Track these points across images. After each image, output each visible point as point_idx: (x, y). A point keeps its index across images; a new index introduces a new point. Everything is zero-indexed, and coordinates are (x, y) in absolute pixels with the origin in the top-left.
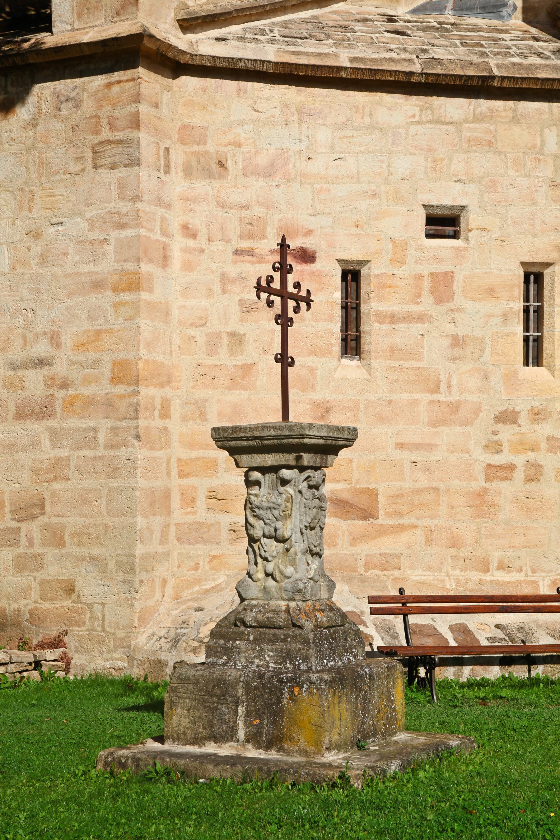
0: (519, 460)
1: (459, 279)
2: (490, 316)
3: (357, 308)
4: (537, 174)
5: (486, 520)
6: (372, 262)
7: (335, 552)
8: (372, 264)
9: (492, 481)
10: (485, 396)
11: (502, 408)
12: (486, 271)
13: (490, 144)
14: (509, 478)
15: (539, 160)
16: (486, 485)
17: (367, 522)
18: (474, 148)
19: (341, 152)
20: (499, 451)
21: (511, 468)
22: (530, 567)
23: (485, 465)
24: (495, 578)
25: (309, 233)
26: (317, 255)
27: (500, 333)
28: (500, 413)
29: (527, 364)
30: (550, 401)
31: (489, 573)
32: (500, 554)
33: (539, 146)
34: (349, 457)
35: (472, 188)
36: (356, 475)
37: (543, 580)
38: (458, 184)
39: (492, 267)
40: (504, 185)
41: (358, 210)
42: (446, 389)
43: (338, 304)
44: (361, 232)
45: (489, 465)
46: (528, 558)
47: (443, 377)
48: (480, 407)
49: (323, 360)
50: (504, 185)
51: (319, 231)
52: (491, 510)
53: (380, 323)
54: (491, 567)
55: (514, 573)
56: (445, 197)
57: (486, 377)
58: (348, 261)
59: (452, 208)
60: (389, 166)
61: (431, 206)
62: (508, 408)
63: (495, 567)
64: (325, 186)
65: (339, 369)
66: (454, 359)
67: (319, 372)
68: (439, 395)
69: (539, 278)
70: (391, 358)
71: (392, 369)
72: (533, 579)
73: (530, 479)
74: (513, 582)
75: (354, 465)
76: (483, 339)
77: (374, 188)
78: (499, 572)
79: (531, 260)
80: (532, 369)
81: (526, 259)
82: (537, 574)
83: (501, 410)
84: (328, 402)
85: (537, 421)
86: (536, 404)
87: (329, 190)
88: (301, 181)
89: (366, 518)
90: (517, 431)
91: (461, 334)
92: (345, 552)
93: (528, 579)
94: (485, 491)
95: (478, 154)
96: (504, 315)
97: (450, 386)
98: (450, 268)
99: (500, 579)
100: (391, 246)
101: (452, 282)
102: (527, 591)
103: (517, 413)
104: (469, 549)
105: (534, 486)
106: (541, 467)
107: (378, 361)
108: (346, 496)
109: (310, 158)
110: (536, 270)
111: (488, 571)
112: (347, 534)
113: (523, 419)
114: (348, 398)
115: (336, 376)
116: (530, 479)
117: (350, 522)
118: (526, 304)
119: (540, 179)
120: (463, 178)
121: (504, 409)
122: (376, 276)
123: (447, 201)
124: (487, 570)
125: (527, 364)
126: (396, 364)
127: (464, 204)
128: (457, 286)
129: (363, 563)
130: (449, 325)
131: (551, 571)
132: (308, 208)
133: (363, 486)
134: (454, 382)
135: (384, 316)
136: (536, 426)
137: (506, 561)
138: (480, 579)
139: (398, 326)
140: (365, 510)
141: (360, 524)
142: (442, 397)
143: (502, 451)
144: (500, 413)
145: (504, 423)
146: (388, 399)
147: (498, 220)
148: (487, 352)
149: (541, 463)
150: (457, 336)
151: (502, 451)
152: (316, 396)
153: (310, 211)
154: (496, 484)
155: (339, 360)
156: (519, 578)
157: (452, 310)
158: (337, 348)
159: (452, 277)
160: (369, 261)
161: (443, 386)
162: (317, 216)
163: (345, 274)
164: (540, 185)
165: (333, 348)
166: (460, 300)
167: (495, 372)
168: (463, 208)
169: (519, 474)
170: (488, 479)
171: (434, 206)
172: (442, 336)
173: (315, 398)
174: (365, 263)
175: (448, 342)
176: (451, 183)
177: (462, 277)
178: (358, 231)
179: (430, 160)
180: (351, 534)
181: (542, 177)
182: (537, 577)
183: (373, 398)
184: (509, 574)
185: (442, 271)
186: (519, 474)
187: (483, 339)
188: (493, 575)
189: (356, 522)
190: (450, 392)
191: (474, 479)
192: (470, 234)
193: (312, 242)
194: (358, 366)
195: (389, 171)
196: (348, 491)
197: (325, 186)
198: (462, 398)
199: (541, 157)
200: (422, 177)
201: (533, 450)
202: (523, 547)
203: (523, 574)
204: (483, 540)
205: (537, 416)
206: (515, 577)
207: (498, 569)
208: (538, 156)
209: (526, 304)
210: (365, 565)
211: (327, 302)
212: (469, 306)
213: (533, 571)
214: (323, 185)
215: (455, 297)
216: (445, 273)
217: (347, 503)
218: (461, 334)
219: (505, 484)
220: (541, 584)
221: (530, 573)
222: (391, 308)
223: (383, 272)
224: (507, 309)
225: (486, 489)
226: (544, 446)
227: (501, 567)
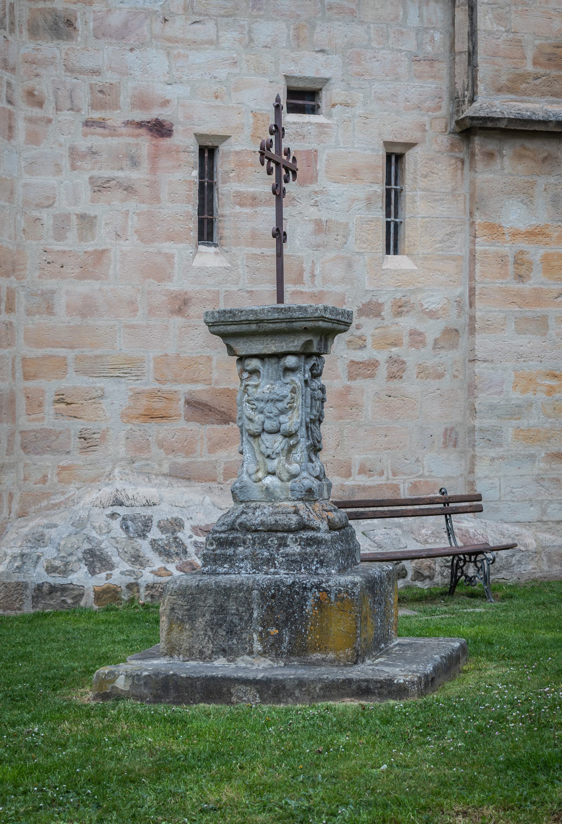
0: (382, 356)
1: (323, 157)
2: (354, 200)
3: (211, 186)
4: (400, 47)
5: (349, 421)
6: (232, 138)
7: (193, 460)
8: (232, 140)
9: (355, 379)
10: (349, 287)
11: (366, 300)
12: (349, 150)
13: (352, 12)
14: (372, 376)
15: (402, 33)
16: (349, 383)
17: (227, 426)
18: (337, 16)
19: (200, 14)
20: (362, 347)
21: (374, 364)
22: (391, 469)
23: (348, 362)
24: (357, 483)
25: (166, 103)
26: (174, 128)
27: (364, 218)
28: (363, 305)
29: (388, 252)
30: (413, 292)
31: (351, 478)
32: (362, 457)
33: (401, 17)
34: (208, 355)
35: (336, 59)
36: (215, 375)
37: (404, 483)
38: (319, 55)
39: (356, 146)
40: (368, 58)
41: (217, 80)
42: (310, 279)
43: (195, 184)
44: (221, 104)
45: (352, 361)
46: (389, 461)
47: (307, 266)
48: (344, 298)
49: (181, 246)
50: (368, 58)
51: (176, 101)
52: (354, 410)
53: (241, 205)
54: (353, 471)
55: (376, 476)
56: (308, 67)
57: (350, 265)
58: (206, 136)
59: (314, 80)
60: (250, 32)
61: (293, 77)
62: (371, 300)
63: (357, 471)
64: (182, 51)
65: (197, 256)
66: (317, 247)
67: (176, 259)
68: (302, 286)
69: (400, 157)
70: (252, 244)
71: (254, 257)
72: (395, 482)
73: (392, 377)
74: (374, 487)
75: (214, 363)
76: (347, 224)
77: (235, 55)
78: (360, 476)
79: (395, 140)
80: (391, 257)
81: (390, 138)
82: (398, 478)
83: (364, 302)
84: (186, 293)
85: (399, 314)
86: (399, 295)
87: (187, 56)
88: (157, 46)
89: (226, 422)
90: (380, 325)
91: (324, 219)
92: (204, 459)
93: (389, 482)
94: (348, 389)
95: (340, 23)
96: (369, 199)
97: (313, 276)
98: (314, 146)
99: (361, 483)
100: (251, 121)
101: (316, 161)
102: (388, 495)
103: (382, 304)
104: (332, 452)
105: (395, 384)
106: (404, 363)
107: (239, 248)
108: (205, 398)
109: (166, 20)
110: (397, 150)
111: (350, 476)
112: (206, 440)
113: (387, 311)
114: (208, 288)
115: (194, 264)
116: (392, 377)
117: (209, 427)
118: (388, 187)
119: (403, 53)
120: (326, 48)
121: (368, 300)
122: (237, 153)
123: (310, 73)
124: (348, 475)
125: (388, 252)
126: (258, 251)
127: (327, 77)
128: (321, 166)
129: (222, 471)
130: (312, 209)
131: (412, 474)
132: (164, 76)
133: (222, 386)
134: (317, 272)
135: (245, 197)
136: (398, 320)
137: (368, 465)
138: (342, 485)
139: (259, 209)
140: (225, 413)
141: (221, 429)
142: (305, 289)
143: (365, 346)
144: (363, 305)
145: (367, 316)
146: (249, 289)
147: (362, 95)
148: (351, 239)
149: (404, 359)
150: (320, 220)
151: (365, 346)
152: (173, 286)
153: (167, 79)
154: (358, 383)
155: (197, 248)
156: (380, 482)
157: (316, 192)
158: (194, 234)
159: (316, 156)
160: (229, 137)
161: (306, 275)
162: (174, 85)
163: (202, 150)
164: (403, 59)
165: (192, 234)
166: (323, 182)
167: (359, 260)
168: (327, 80)
169: (383, 371)
170: (351, 377)
171: (296, 77)
172: (305, 220)
173: (172, 289)
174: (225, 138)
175: (311, 227)
176: (314, 53)
177: (325, 157)
178: (218, 103)
179: (292, 27)
180: (210, 439)
181: (405, 51)
182: (397, 480)
183: (234, 288)
184: (371, 479)
185: (305, 149)
186: (383, 371)
187: (347, 224)
188: (354, 480)
189: (215, 426)
190: (313, 282)
191: (338, 377)
192: (334, 110)
193: (169, 113)
194: (216, 253)
195: (250, 37)
196: (207, 391)
197: (182, 51)
198: (325, 289)
199: (404, 30)
200: (284, 45)
201: (395, 345)
202: (385, 449)
203: (384, 478)
204: (346, 443)
205: (400, 308)
206: (376, 481)
207: (359, 473)
208: (401, 28)
209: (388, 187)
210: (224, 473)
211: (185, 181)
212: (333, 188)
213: (394, 474)
214: (180, 50)
215: (319, 178)
216: (308, 152)
217: (206, 405)
218: (324, 219)
219: (368, 382)
220: (401, 487)
221: (391, 476)
222: (252, 189)
223: (244, 148)
224: (371, 193)
225: (349, 387)
226: (406, 340)
227: (363, 470)
